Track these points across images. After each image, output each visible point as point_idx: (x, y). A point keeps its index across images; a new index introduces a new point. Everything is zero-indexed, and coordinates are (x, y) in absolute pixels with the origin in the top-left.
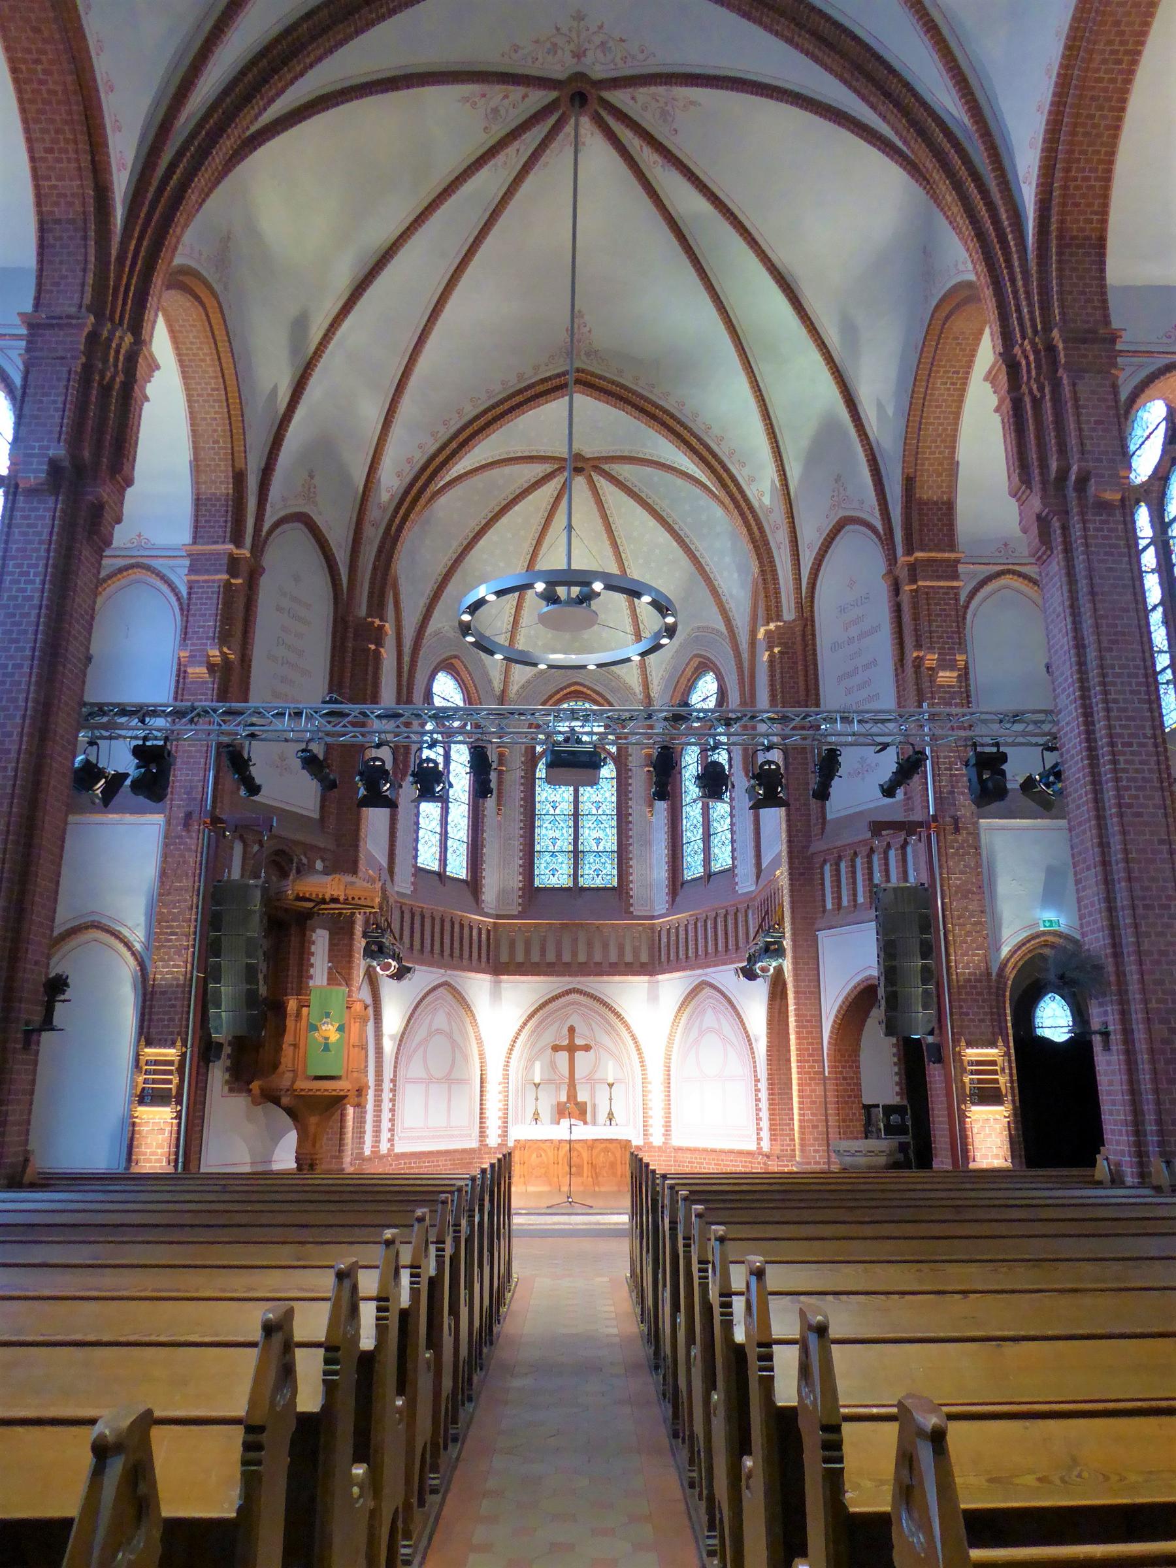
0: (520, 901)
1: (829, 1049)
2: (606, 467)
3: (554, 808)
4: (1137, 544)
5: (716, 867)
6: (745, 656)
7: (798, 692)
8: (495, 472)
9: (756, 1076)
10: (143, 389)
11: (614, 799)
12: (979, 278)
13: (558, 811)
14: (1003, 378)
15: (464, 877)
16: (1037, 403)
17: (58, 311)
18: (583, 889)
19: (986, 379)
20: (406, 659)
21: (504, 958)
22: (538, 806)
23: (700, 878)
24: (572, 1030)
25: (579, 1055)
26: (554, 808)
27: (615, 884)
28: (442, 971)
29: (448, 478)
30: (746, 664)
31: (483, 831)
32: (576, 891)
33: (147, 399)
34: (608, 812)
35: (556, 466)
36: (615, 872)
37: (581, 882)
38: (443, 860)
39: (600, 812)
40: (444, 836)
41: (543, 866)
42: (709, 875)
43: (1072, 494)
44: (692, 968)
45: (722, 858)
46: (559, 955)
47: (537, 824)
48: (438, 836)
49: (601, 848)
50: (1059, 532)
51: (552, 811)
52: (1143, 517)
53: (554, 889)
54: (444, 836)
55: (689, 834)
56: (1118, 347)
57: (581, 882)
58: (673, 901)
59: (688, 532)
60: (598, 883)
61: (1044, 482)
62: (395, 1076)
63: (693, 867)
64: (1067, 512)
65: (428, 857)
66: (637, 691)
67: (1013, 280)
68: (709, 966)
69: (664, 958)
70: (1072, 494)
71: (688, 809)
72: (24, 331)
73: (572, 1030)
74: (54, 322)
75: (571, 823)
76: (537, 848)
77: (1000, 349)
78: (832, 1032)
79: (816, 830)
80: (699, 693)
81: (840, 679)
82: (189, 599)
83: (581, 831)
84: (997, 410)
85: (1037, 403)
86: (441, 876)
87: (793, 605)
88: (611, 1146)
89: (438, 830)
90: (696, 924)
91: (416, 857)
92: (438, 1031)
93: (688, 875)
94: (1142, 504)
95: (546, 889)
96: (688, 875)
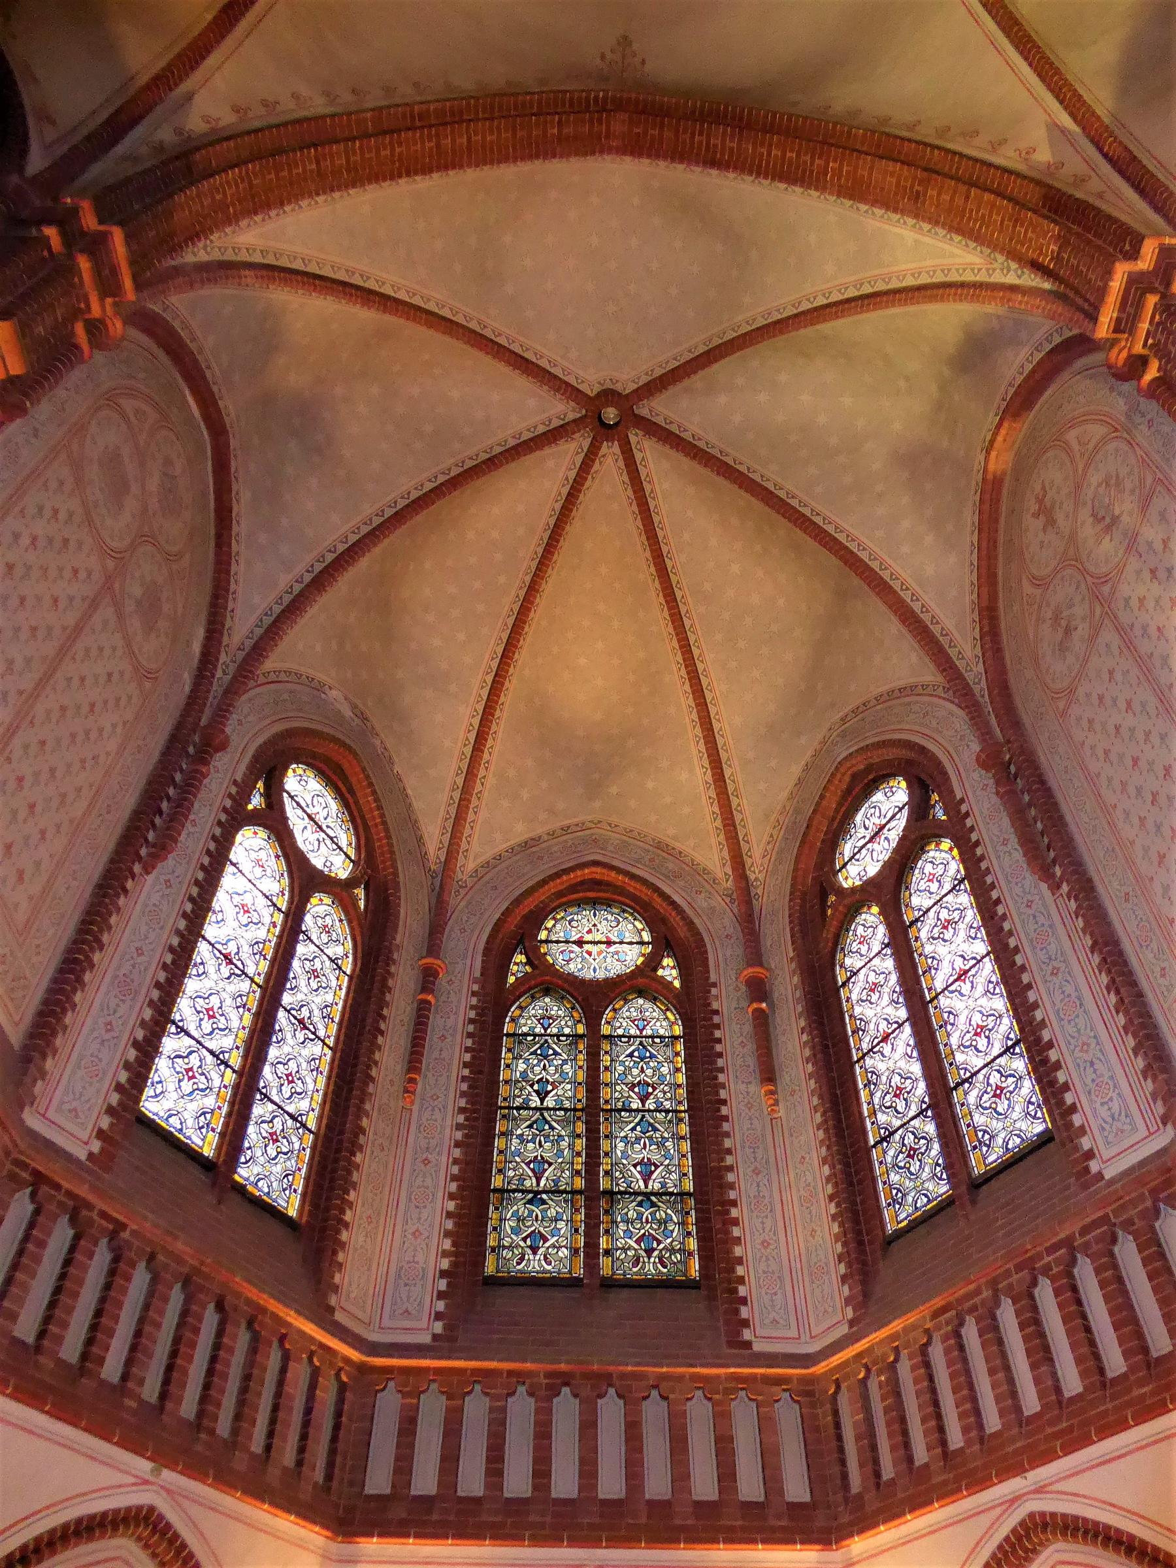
0: (441, 1306)
3: (542, 1095)
11: (681, 1078)
15: (292, 1212)
18: (609, 1284)
21: (378, 1481)
22: (503, 1090)
23: (945, 1205)
26: (542, 1095)
28: (144, 1466)
30: (980, 688)
31: (360, 1112)
34: (667, 1105)
36: (692, 1244)
41: (508, 1226)
47: (499, 1127)
48: (230, 1077)
49: (654, 1185)
51: (535, 1101)
55: (882, 1118)
58: (866, 1295)
66: (719, 874)
68: (1048, 1457)
71: (869, 1062)
75: (581, 1128)
76: (497, 1182)
80: (862, 832)
83: (605, 1145)
89: (235, 1059)
93: (895, 1218)
96: (895, 1218)
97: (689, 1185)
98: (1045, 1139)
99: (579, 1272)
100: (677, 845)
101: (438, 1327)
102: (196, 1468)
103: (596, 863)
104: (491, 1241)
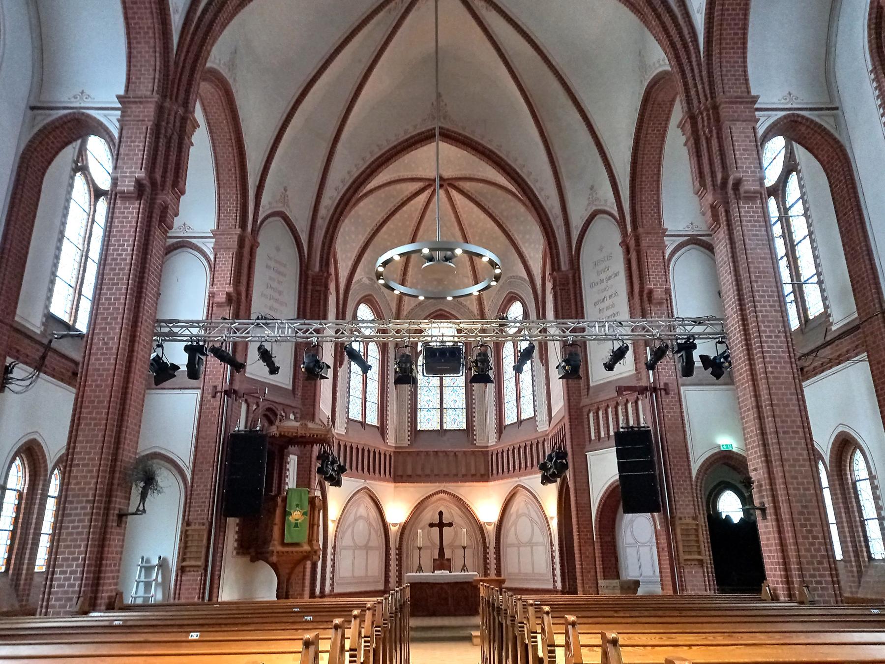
1: (596, 524)
2: (456, 184)
4: (770, 221)
5: (524, 416)
6: (539, 292)
7: (571, 312)
8: (392, 187)
9: (551, 543)
10: (190, 138)
12: (672, 69)
13: (430, 385)
14: (688, 127)
15: (376, 424)
16: (708, 140)
17: (139, 93)
19: (678, 127)
20: (341, 296)
23: (516, 423)
24: (441, 514)
25: (445, 529)
27: (465, 428)
29: (365, 191)
32: (442, 432)
33: (192, 145)
35: (427, 184)
37: (445, 428)
38: (364, 415)
39: (455, 385)
40: (365, 400)
42: (520, 422)
43: (730, 192)
44: (512, 477)
45: (527, 412)
46: (432, 471)
47: (419, 391)
49: (456, 406)
50: (724, 214)
51: (427, 385)
52: (772, 203)
53: (429, 430)
54: (365, 400)
56: (756, 106)
57: (445, 428)
59: (505, 221)
60: (455, 427)
61: (714, 185)
62: (335, 545)
63: (510, 417)
64: (728, 203)
65: (355, 413)
66: (476, 314)
67: (692, 70)
69: (495, 472)
70: (730, 192)
72: (119, 106)
73: (441, 514)
74: (137, 100)
76: (419, 406)
77: (686, 109)
78: (597, 514)
79: (584, 392)
81: (596, 304)
82: (215, 261)
84: (685, 144)
85: (708, 140)
86: (363, 424)
87: (567, 262)
88: (465, 586)
89: (361, 397)
90: (513, 450)
91: (348, 412)
92: (361, 517)
94: (772, 197)
95: (424, 431)
97: (464, 406)
98: (532, 418)
99: (439, 428)
100: (465, 303)
101: (409, 443)
102: (371, 479)
103: (441, 310)
104: (418, 421)
